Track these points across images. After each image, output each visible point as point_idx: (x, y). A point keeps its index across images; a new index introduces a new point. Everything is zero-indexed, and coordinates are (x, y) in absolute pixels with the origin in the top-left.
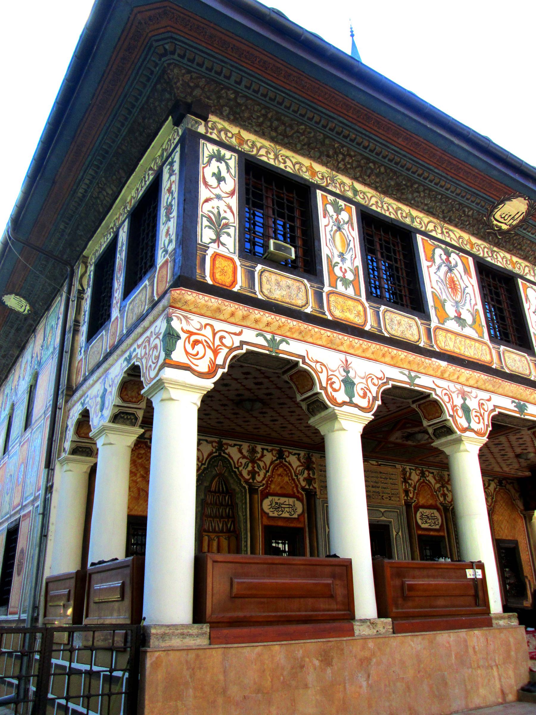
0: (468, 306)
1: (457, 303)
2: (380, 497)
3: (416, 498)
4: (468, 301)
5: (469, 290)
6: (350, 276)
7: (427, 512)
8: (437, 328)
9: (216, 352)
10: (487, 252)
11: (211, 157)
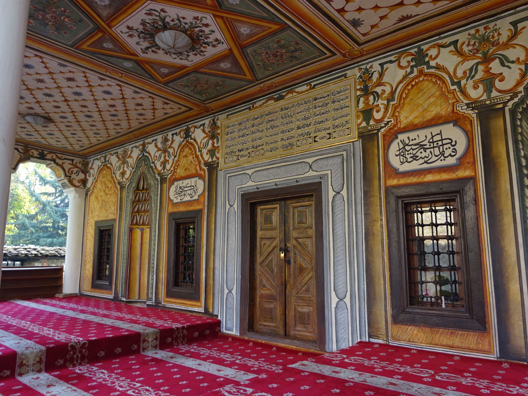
2: (310, 140)
3: (393, 115)
7: (421, 135)
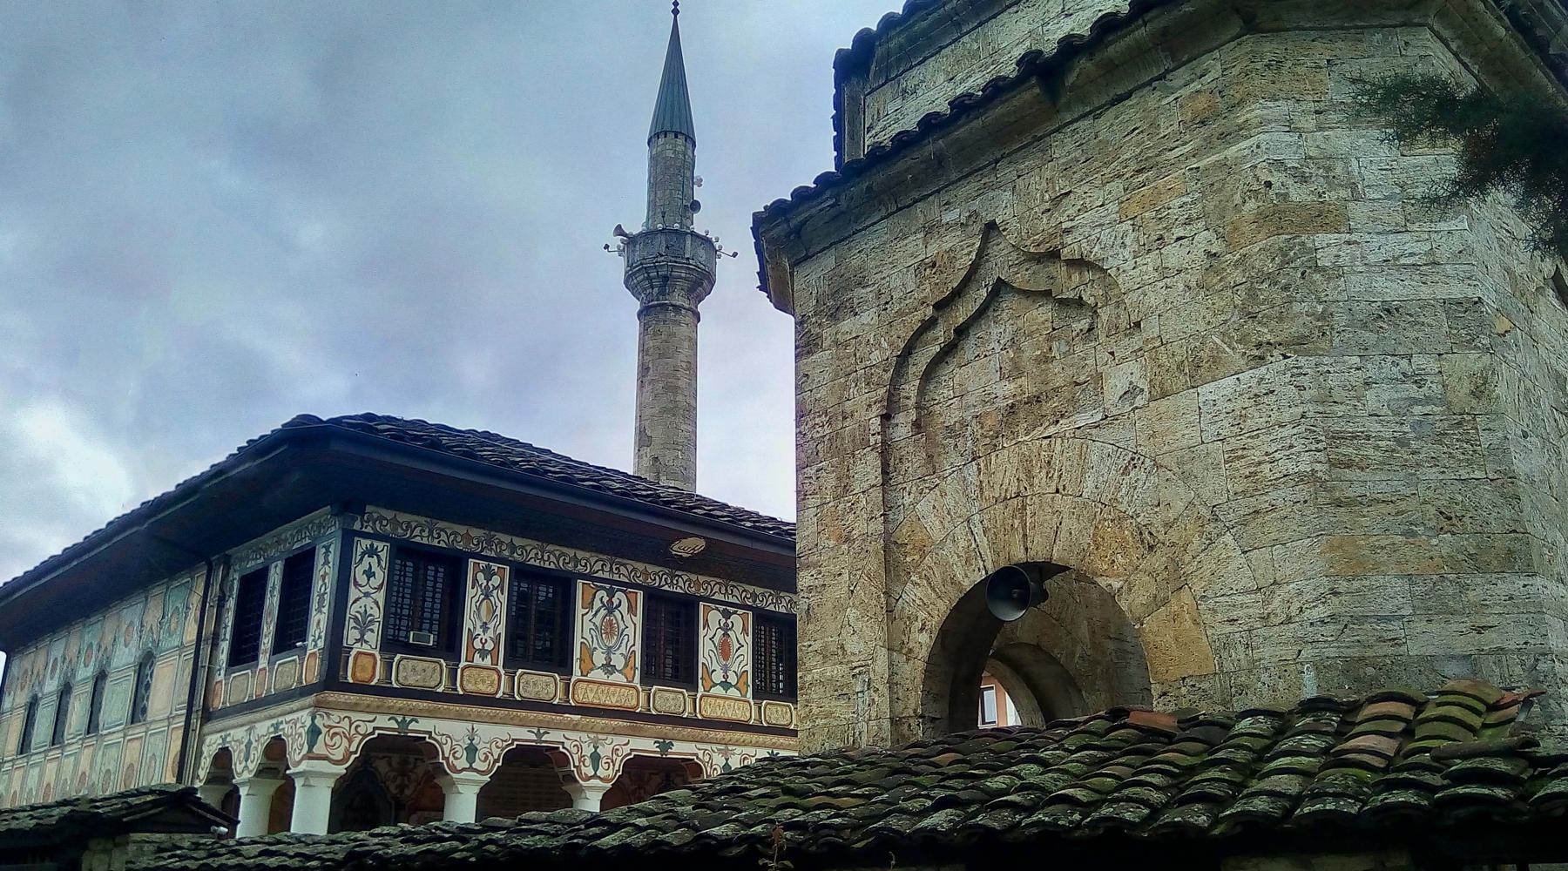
0: (623, 650)
1: (609, 651)
5: (630, 631)
6: (489, 646)
9: (350, 742)
11: (363, 554)
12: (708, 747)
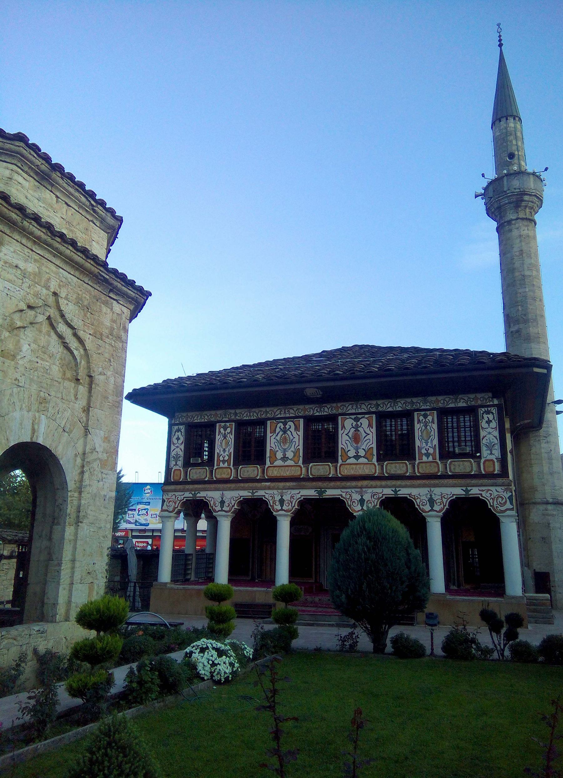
0: (292, 449)
1: (285, 451)
4: (293, 446)
8: (269, 467)
9: (175, 504)
10: (317, 410)
12: (349, 490)
